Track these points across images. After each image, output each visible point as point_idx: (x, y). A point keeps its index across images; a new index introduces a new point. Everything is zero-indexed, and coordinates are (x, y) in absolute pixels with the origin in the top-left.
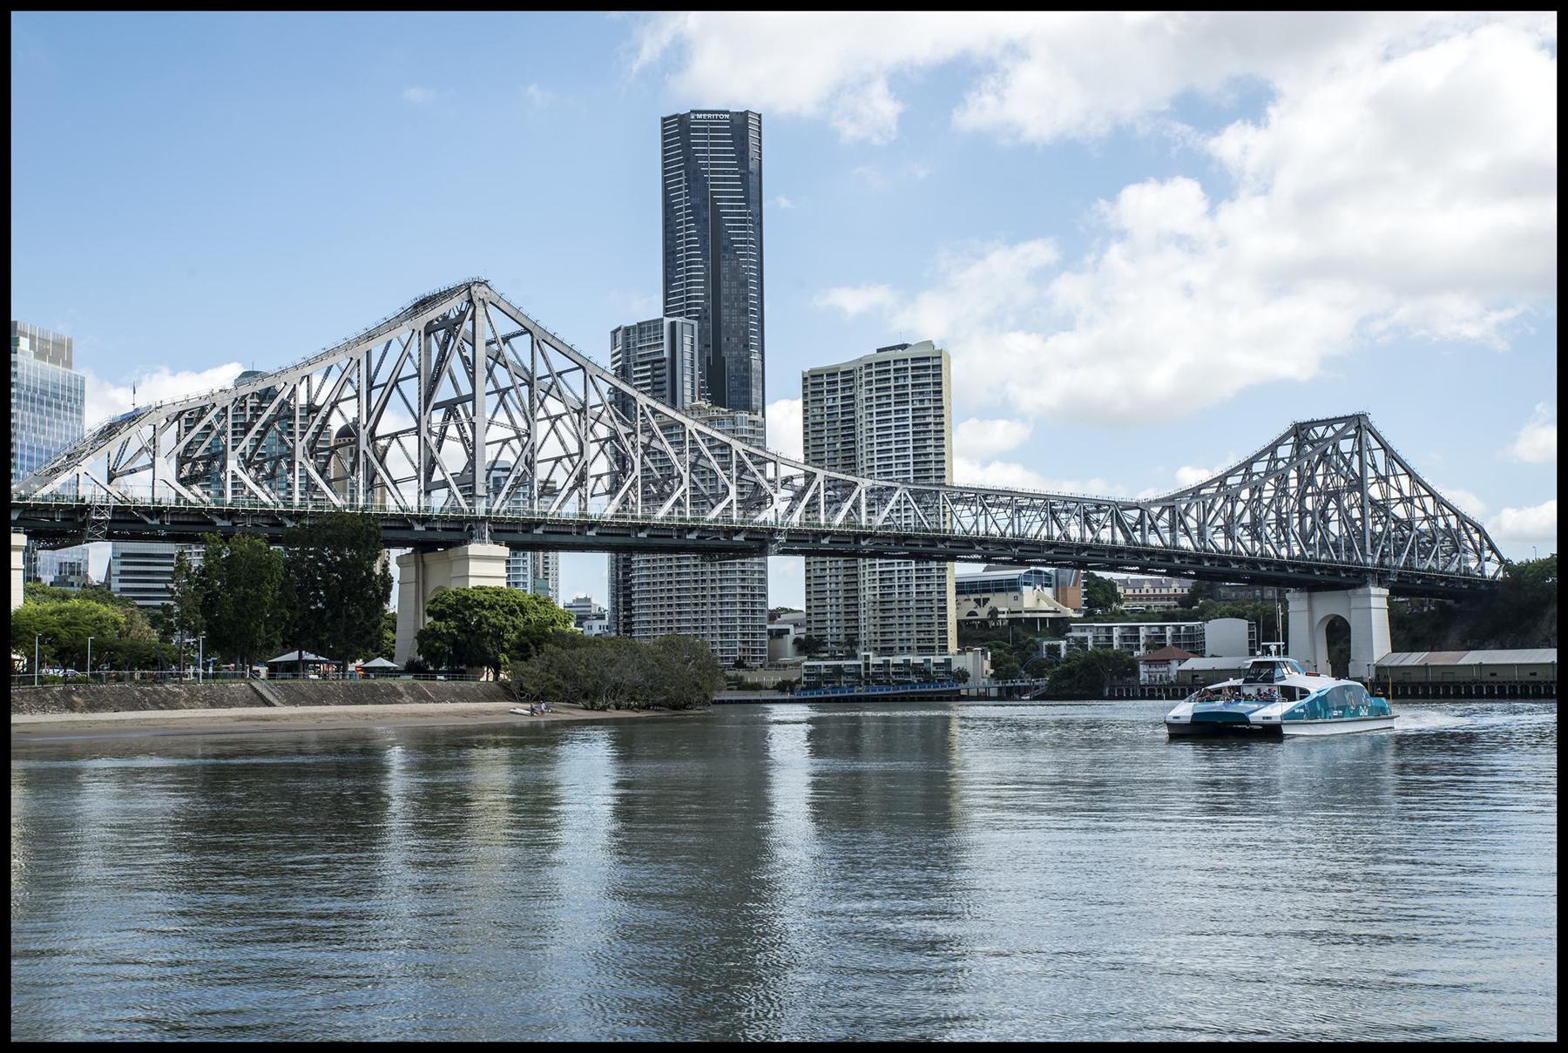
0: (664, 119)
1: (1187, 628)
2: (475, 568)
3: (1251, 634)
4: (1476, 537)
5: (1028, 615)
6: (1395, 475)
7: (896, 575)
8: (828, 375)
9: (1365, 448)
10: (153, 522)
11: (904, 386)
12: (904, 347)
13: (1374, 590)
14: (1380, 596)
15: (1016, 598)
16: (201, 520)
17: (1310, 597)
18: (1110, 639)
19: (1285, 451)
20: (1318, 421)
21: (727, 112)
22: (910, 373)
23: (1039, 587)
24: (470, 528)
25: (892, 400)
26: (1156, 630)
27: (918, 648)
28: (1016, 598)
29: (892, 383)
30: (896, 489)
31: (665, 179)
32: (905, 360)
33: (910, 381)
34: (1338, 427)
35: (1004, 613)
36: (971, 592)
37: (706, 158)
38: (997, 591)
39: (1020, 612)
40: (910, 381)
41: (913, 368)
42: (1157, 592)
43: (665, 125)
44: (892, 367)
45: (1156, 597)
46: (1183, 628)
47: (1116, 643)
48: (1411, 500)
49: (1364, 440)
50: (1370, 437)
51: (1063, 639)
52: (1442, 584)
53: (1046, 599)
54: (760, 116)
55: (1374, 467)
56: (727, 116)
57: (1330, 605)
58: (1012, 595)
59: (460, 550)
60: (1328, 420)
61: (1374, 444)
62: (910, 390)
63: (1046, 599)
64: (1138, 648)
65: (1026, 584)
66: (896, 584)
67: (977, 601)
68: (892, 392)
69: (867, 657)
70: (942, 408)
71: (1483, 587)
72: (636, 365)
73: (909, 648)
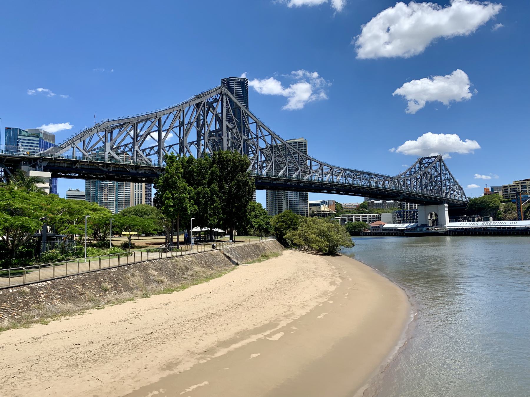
0: (222, 80)
1: (373, 216)
5: (323, 212)
10: (105, 170)
12: (295, 139)
15: (319, 208)
16: (124, 170)
17: (425, 207)
19: (418, 166)
22: (298, 146)
23: (324, 205)
28: (319, 208)
34: (433, 159)
37: (234, 90)
38: (314, 206)
47: (354, 220)
55: (443, 170)
56: (239, 79)
58: (319, 207)
61: (443, 165)
63: (326, 208)
64: (367, 221)
66: (294, 204)
71: (463, 204)
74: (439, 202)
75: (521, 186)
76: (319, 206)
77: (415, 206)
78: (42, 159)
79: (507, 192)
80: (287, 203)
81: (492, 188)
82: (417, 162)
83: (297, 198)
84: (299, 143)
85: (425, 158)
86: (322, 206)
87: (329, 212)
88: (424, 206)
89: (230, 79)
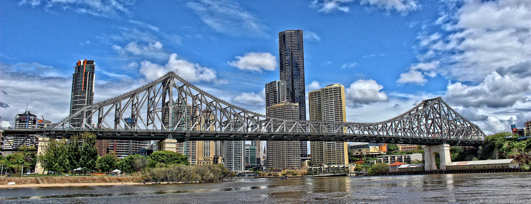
2: (167, 145)
5: (371, 154)
6: (451, 114)
8: (314, 93)
9: (441, 106)
13: (445, 145)
15: (368, 149)
18: (388, 160)
20: (429, 100)
21: (294, 30)
24: (167, 135)
25: (329, 99)
26: (400, 157)
27: (337, 163)
30: (295, 122)
35: (365, 153)
36: (357, 148)
39: (369, 153)
41: (334, 90)
43: (280, 36)
44: (329, 90)
46: (407, 156)
48: (456, 120)
49: (440, 104)
50: (442, 104)
52: (467, 143)
53: (377, 149)
54: (302, 31)
56: (294, 31)
57: (434, 149)
58: (367, 148)
59: (163, 141)
60: (431, 99)
61: (444, 105)
67: (359, 150)
69: (324, 166)
70: (341, 100)
72: (271, 93)
73: (335, 163)
74: (439, 142)
76: (368, 147)
82: (421, 104)
86: (371, 147)
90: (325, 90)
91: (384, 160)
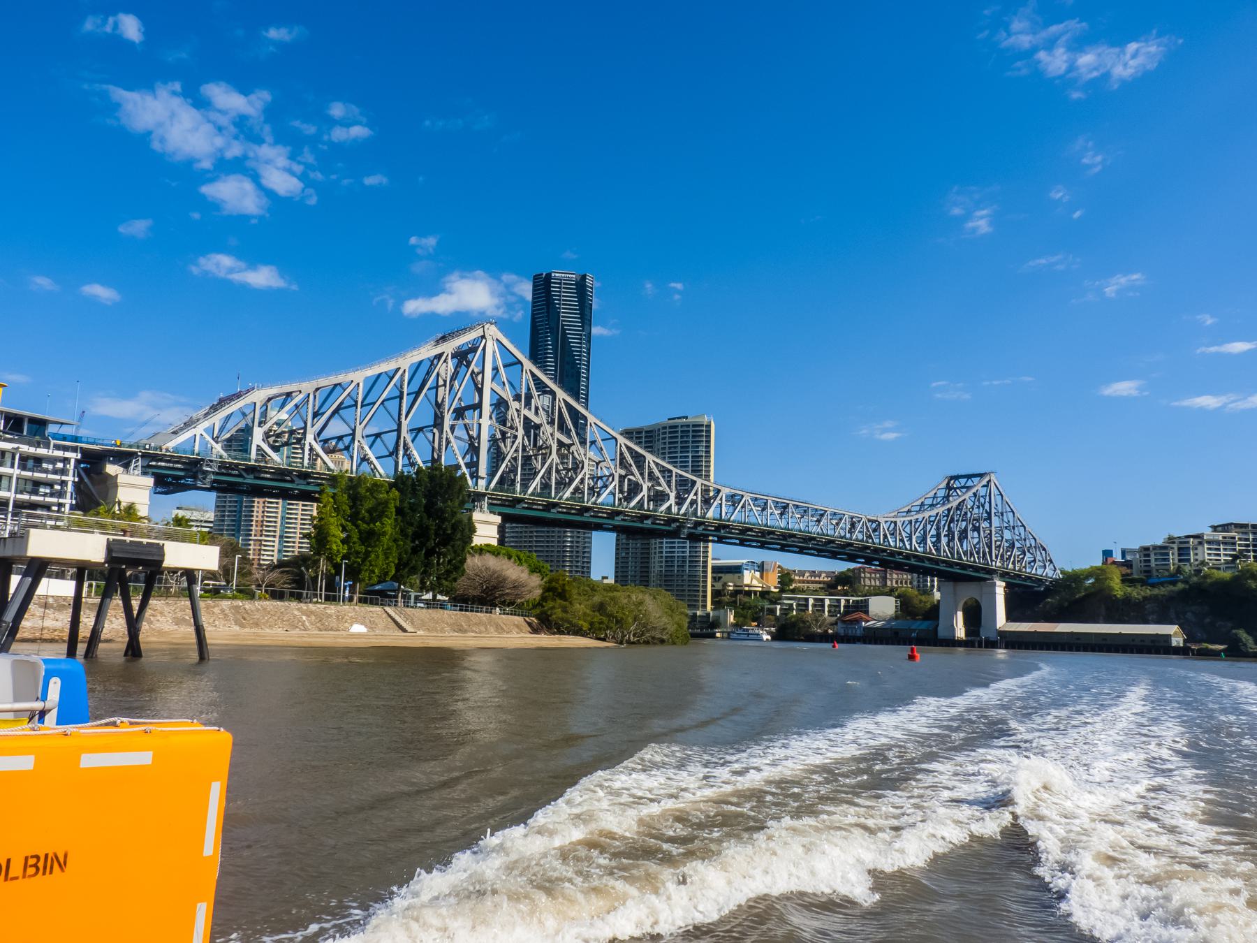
3: (896, 606)
4: (1043, 553)
5: (747, 589)
7: (676, 559)
11: (686, 442)
12: (686, 418)
14: (1000, 586)
15: (739, 578)
23: (753, 571)
29: (679, 440)
31: (533, 311)
32: (688, 426)
33: (691, 439)
40: (691, 439)
42: (813, 578)
44: (679, 429)
45: (813, 582)
51: (778, 604)
53: (756, 578)
57: (968, 592)
62: (690, 445)
63: (756, 578)
65: (746, 569)
68: (679, 445)
75: (1179, 549)
77: (932, 581)
78: (140, 454)
79: (1149, 561)
80: (661, 562)
81: (1124, 553)
83: (683, 552)
84: (694, 426)
85: (956, 478)
86: (746, 573)
87: (760, 589)
88: (951, 583)
89: (553, 275)
90: (671, 427)
91: (798, 605)
